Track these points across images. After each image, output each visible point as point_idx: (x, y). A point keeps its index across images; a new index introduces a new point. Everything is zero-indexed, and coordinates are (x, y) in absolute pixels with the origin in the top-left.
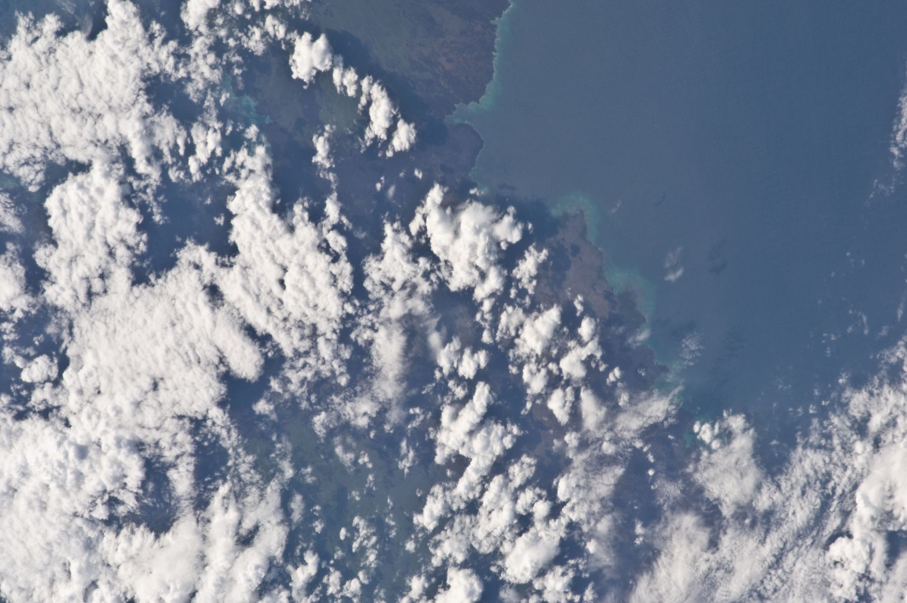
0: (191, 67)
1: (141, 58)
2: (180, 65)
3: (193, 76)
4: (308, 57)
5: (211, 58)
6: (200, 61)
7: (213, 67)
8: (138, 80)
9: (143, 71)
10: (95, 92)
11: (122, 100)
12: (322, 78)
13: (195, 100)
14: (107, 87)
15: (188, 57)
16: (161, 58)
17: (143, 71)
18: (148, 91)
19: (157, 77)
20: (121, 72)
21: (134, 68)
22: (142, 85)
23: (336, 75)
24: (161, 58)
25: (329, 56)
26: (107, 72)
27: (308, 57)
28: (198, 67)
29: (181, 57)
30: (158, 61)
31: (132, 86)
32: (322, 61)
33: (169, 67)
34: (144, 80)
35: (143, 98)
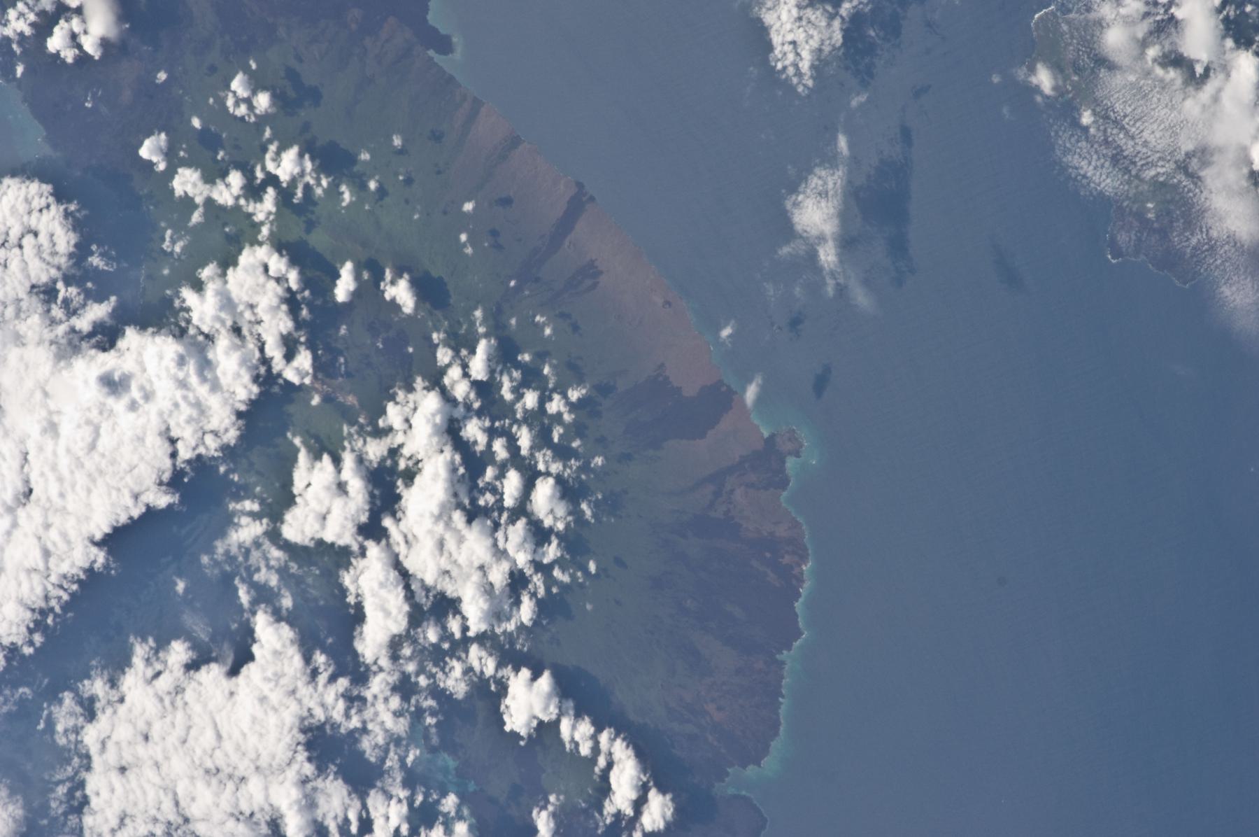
0: (368, 714)
1: (300, 701)
2: (353, 711)
3: (370, 726)
4: (526, 701)
5: (395, 702)
6: (380, 707)
7: (397, 714)
8: (295, 731)
9: (303, 719)
10: (238, 747)
11: (273, 757)
12: (546, 731)
13: (373, 759)
14: (253, 740)
15: (363, 700)
16: (328, 701)
17: (303, 719)
18: (309, 746)
19: (321, 727)
20: (272, 719)
21: (290, 714)
22: (301, 738)
23: (565, 726)
24: (328, 701)
25: (556, 700)
26: (254, 720)
27: (526, 701)
28: (376, 714)
29: (354, 700)
30: (323, 705)
31: (288, 739)
32: (546, 708)
33: (337, 714)
34: (304, 731)
35: (302, 755)
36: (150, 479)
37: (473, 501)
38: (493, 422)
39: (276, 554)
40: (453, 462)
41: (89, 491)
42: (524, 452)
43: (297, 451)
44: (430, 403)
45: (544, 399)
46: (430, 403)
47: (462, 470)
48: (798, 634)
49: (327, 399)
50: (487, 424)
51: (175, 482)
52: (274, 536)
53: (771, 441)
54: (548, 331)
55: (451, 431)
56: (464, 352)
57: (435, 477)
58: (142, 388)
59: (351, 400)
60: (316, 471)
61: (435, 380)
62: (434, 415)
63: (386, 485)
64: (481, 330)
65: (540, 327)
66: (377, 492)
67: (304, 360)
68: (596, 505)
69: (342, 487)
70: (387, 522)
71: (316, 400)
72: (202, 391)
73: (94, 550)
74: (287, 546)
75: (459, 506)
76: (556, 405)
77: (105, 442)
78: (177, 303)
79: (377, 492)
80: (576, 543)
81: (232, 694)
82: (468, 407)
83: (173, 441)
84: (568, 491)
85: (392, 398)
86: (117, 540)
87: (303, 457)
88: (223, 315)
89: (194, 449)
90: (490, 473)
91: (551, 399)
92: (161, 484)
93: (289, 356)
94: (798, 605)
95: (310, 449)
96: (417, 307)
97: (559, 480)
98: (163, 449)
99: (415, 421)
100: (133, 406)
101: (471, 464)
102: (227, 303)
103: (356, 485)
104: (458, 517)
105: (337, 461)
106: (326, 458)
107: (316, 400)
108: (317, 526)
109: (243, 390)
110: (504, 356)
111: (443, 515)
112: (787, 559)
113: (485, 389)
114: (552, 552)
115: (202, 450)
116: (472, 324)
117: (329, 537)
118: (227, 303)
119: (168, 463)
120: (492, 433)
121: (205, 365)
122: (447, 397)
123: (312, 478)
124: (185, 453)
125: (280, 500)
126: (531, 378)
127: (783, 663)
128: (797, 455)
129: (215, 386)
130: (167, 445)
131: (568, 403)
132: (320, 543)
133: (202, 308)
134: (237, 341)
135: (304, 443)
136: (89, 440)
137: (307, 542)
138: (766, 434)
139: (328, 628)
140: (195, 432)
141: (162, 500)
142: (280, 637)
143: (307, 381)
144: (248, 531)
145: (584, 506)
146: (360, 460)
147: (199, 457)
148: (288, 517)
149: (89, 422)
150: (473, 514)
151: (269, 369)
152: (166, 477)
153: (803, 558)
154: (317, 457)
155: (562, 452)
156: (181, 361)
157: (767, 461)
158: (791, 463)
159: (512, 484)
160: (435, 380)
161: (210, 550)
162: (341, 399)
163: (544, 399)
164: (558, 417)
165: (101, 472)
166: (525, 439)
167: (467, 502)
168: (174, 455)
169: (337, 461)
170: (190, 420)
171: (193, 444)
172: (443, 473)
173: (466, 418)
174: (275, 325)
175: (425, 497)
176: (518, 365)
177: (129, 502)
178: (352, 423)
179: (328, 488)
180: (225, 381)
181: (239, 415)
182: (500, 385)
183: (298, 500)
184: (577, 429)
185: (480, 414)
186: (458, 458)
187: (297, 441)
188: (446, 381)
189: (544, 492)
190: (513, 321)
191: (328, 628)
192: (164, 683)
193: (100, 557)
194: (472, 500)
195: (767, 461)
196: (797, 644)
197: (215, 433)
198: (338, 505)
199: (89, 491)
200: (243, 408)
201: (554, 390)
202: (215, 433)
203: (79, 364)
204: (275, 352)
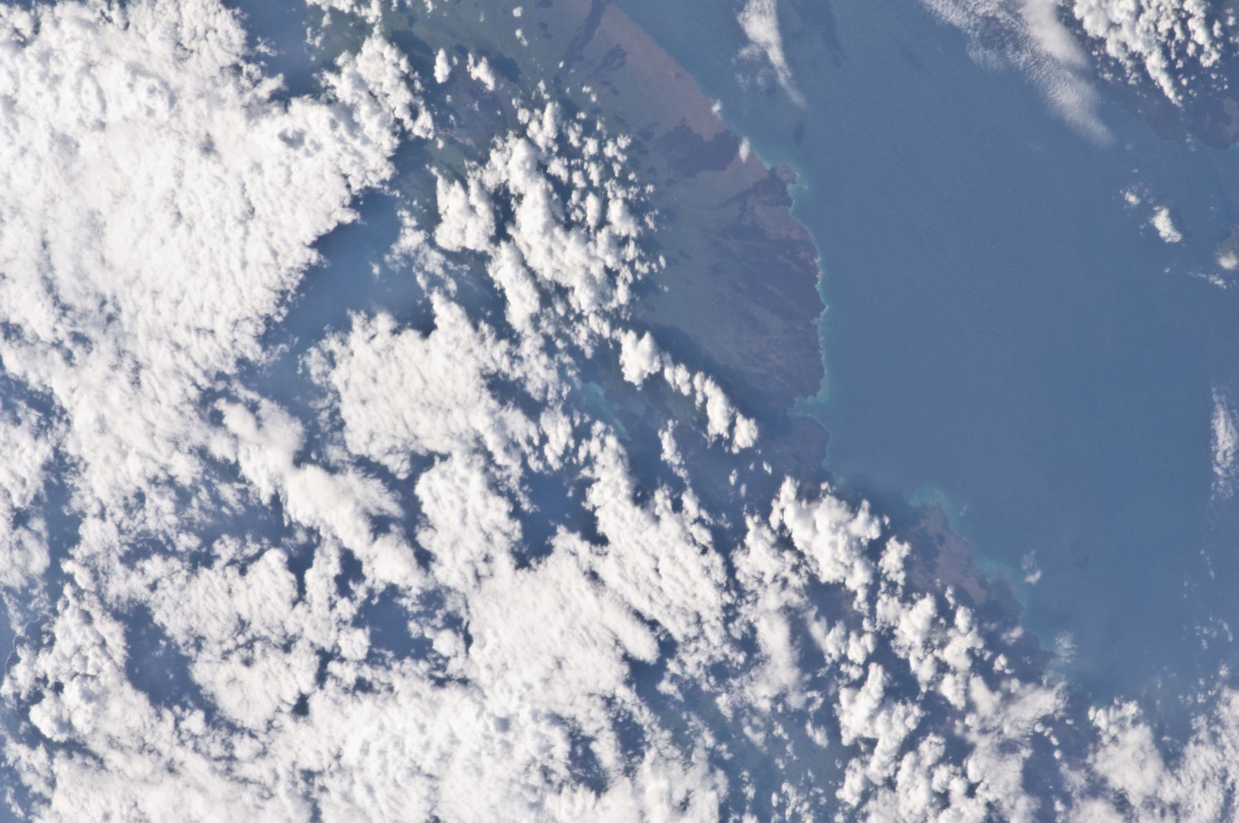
0: (526, 367)
1: (477, 358)
2: (515, 366)
3: (530, 376)
4: (636, 358)
5: (544, 359)
6: (534, 362)
7: (547, 367)
8: (478, 378)
9: (481, 370)
10: (440, 389)
11: (467, 396)
12: (654, 381)
13: (537, 398)
14: (449, 384)
15: (521, 358)
17: (481, 370)
18: (491, 387)
19: (496, 375)
20: (459, 370)
21: (471, 366)
22: (483, 382)
23: (668, 374)
24: (495, 355)
25: (657, 358)
26: (447, 370)
27: (636, 358)
28: (532, 368)
29: (514, 358)
30: (493, 359)
31: (473, 384)
32: (652, 364)
33: (504, 365)
34: (484, 377)
35: (486, 394)
36: (335, 205)
37: (568, 216)
38: (569, 161)
39: (435, 256)
40: (547, 190)
41: (293, 212)
42: (596, 184)
43: (435, 180)
44: (519, 149)
45: (601, 146)
46: (519, 149)
47: (555, 196)
48: (823, 308)
49: (450, 141)
50: (566, 163)
51: (354, 204)
52: (431, 242)
53: (772, 173)
54: (594, 99)
55: (541, 167)
56: (537, 112)
57: (536, 202)
58: (312, 142)
59: (469, 141)
60: (451, 195)
61: (522, 132)
62: (524, 163)
63: (503, 205)
64: (546, 96)
65: (588, 95)
66: (498, 208)
67: (425, 119)
68: (657, 219)
69: (472, 209)
70: (510, 231)
71: (441, 144)
72: (357, 144)
73: (308, 251)
74: (443, 251)
75: (558, 221)
76: (610, 151)
77: (295, 178)
78: (323, 84)
79: (498, 208)
80: (647, 244)
81: (427, 351)
82: (549, 150)
83: (346, 177)
84: (634, 209)
85: (494, 146)
86: (322, 243)
87: (441, 183)
88: (359, 92)
89: (362, 182)
90: (575, 196)
91: (606, 145)
92: (344, 206)
93: (415, 115)
94: (818, 286)
95: (445, 176)
96: (497, 83)
97: (625, 201)
98: (337, 184)
99: (510, 163)
100: (308, 154)
101: (561, 190)
102: (359, 82)
103: (482, 208)
104: (558, 231)
105: (465, 187)
106: (457, 183)
107: (441, 144)
108: (459, 238)
109: (388, 143)
110: (567, 113)
111: (547, 230)
112: (802, 255)
113: (561, 138)
114: (631, 251)
115: (367, 183)
116: (539, 94)
117: (470, 245)
118: (359, 82)
119: (345, 192)
120: (570, 169)
121: (354, 127)
122: (531, 142)
123: (450, 199)
124: (356, 187)
125: (430, 219)
126: (588, 130)
127: (816, 326)
128: (794, 182)
129: (366, 141)
130: (341, 179)
131: (619, 150)
132: (464, 249)
133: (342, 87)
134: (376, 106)
135: (440, 171)
136: (284, 177)
137: (455, 249)
138: (768, 167)
139: (485, 306)
140: (359, 171)
141: (348, 217)
142: (452, 314)
143: (430, 136)
144: (411, 239)
145: (647, 219)
146: (481, 185)
147: (367, 188)
148: (438, 231)
149: (281, 164)
150: (568, 226)
151: (403, 128)
152: (347, 201)
153: (814, 254)
154: (451, 182)
155: (623, 182)
156: (334, 125)
157: (772, 186)
158: (790, 188)
159: (592, 203)
160: (522, 132)
161: (390, 251)
162: (460, 141)
163: (601, 146)
164: (614, 158)
165: (298, 198)
166: (595, 176)
167: (563, 218)
168: (348, 186)
169: (465, 187)
170: (353, 163)
171: (360, 179)
172: (541, 201)
173: (549, 158)
174: (399, 99)
175: (531, 214)
176: (579, 121)
177: (325, 219)
178: (471, 159)
179: (461, 212)
180: (373, 137)
181: (390, 159)
182: (568, 138)
183: (443, 217)
184: (632, 164)
185: (559, 154)
186: (551, 187)
187: (434, 171)
188: (529, 134)
189: (616, 210)
190: (568, 90)
191: (485, 306)
192: (378, 342)
193: (314, 256)
194: (563, 216)
195: (772, 186)
196: (823, 313)
197: (374, 172)
198: (471, 222)
199: (293, 212)
200: (390, 154)
201: (608, 138)
202: (374, 172)
203: (265, 122)
204: (401, 113)
